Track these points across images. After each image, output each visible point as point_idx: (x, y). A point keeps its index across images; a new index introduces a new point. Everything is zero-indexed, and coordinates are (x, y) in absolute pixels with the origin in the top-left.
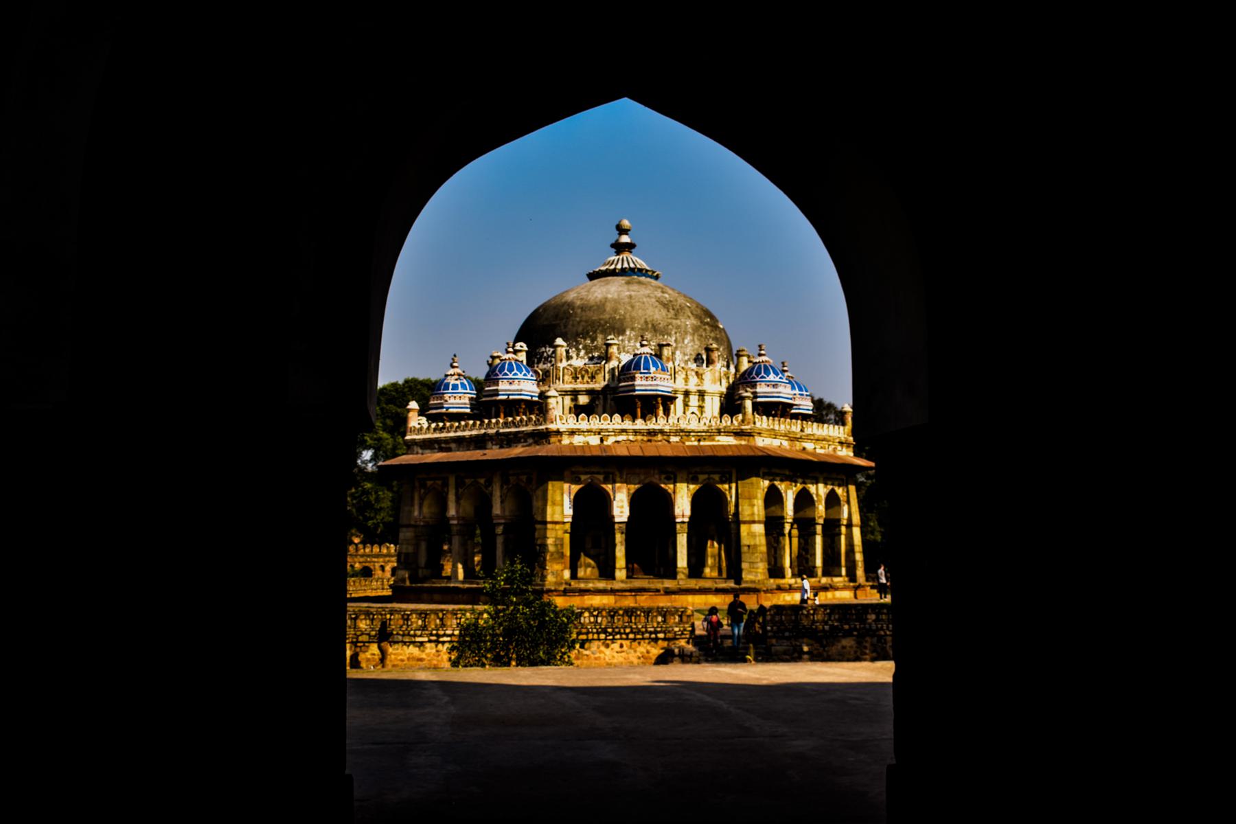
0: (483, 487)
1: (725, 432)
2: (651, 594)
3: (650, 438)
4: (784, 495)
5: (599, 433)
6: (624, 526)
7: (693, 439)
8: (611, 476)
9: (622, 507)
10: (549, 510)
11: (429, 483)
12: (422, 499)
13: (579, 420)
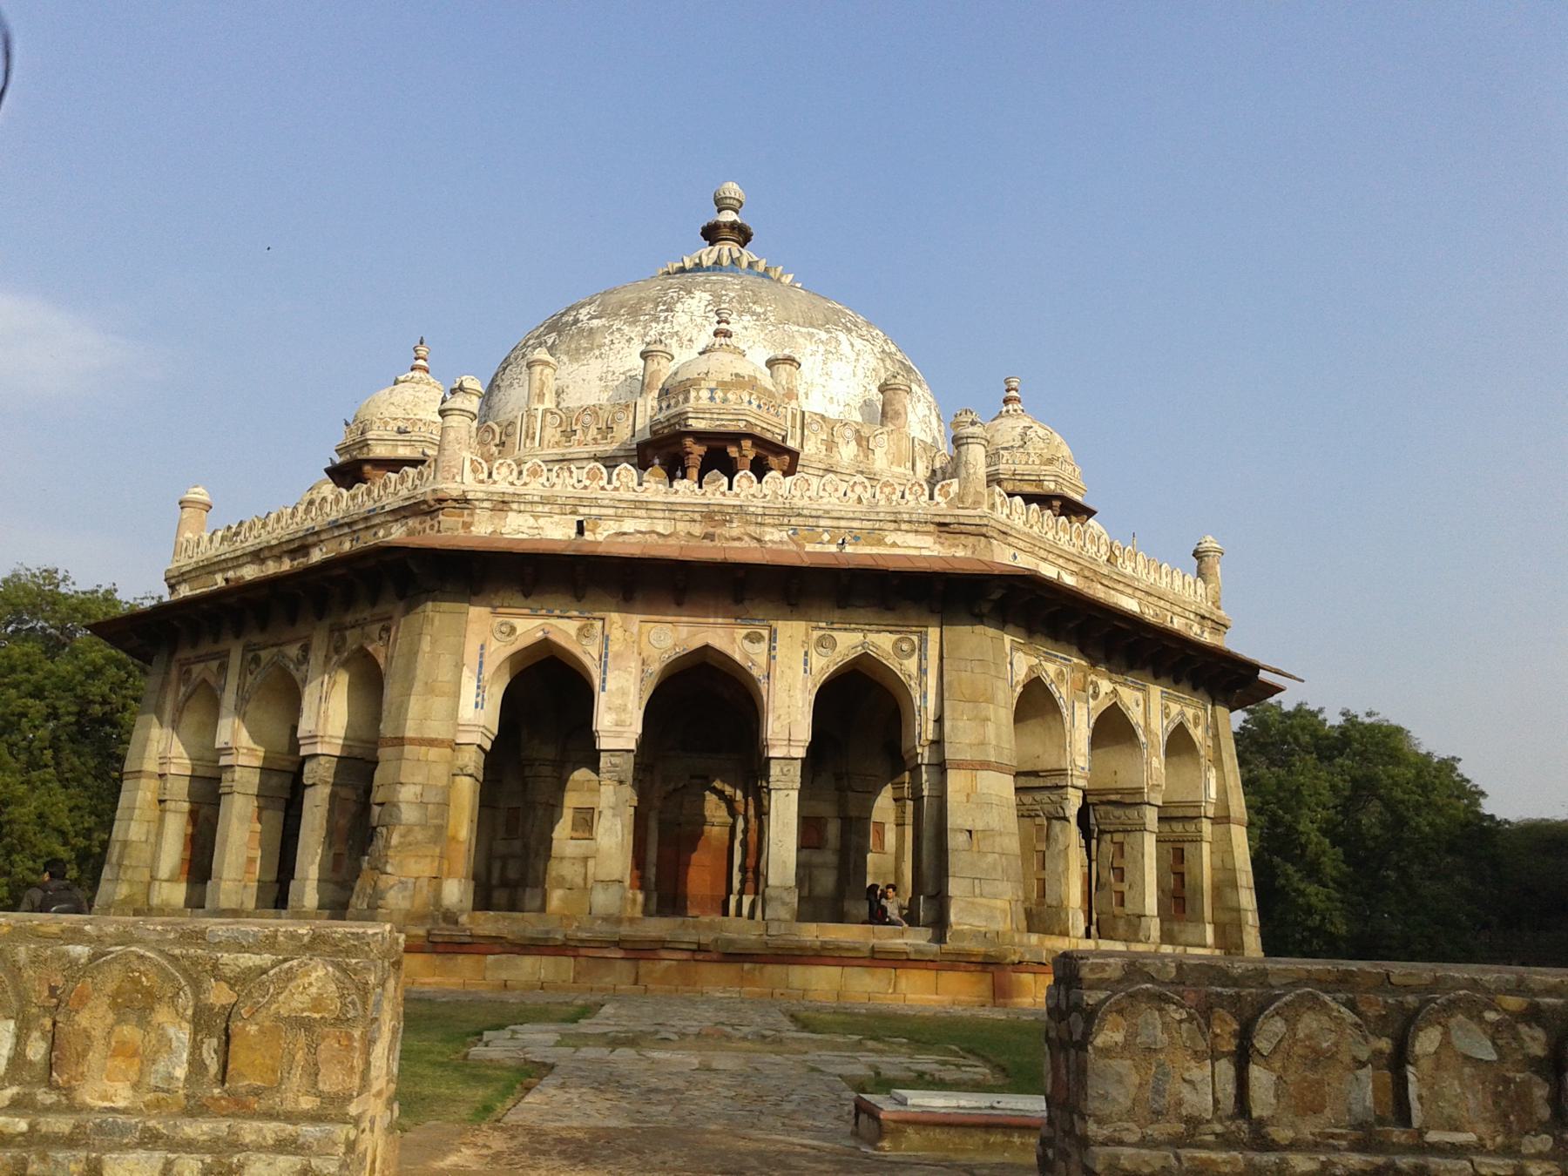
0: (292, 666)
1: (910, 522)
2: (679, 955)
3: (711, 530)
4: (1064, 710)
5: (574, 513)
6: (628, 764)
7: (826, 537)
8: (600, 623)
9: (624, 708)
10: (415, 707)
11: (197, 669)
12: (180, 711)
13: (525, 473)
